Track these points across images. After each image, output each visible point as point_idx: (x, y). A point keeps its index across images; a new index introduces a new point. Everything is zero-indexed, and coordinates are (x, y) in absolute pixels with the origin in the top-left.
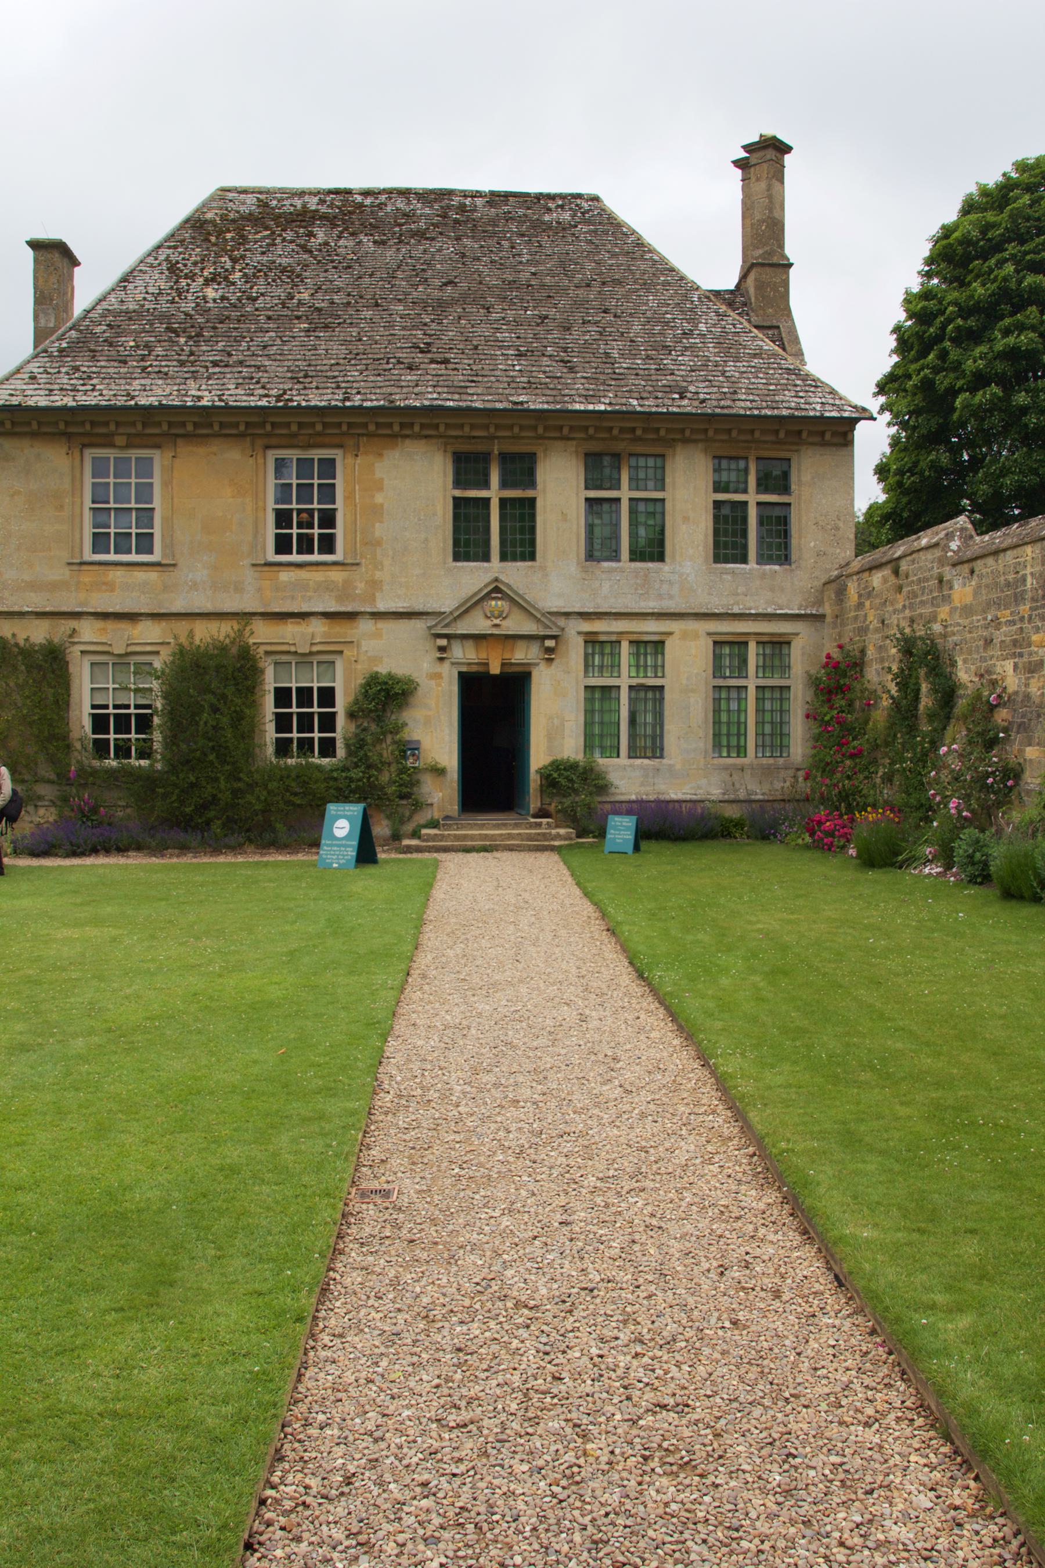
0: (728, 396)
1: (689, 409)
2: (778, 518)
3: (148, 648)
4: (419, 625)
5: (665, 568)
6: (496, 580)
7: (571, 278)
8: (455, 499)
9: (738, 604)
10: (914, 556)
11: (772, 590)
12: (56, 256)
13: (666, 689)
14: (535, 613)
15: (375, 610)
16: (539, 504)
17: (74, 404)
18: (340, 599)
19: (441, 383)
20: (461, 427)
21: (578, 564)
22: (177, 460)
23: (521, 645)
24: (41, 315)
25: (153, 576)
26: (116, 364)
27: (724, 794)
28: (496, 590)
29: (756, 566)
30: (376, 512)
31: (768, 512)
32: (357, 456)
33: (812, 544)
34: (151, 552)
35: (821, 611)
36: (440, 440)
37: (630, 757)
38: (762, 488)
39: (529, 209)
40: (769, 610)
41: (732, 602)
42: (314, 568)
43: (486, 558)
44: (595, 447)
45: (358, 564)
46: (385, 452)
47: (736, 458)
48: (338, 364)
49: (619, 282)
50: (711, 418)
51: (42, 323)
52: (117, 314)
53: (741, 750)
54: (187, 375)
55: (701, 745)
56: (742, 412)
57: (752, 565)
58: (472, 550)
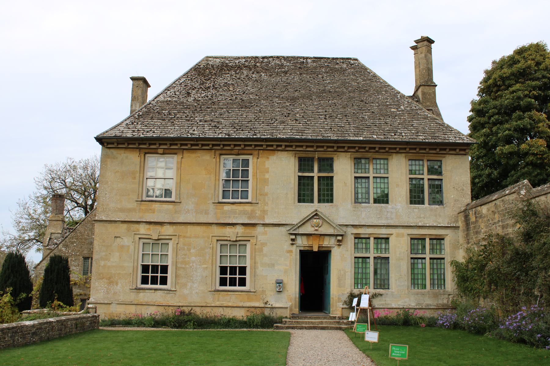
0: (414, 134)
1: (398, 140)
2: (437, 185)
3: (167, 237)
4: (283, 229)
5: (389, 206)
6: (316, 211)
7: (347, 89)
8: (299, 176)
9: (421, 222)
10: (502, 198)
11: (436, 216)
12: (141, 82)
13: (390, 259)
14: (333, 225)
15: (264, 223)
16: (335, 179)
17: (143, 136)
18: (249, 218)
19: (293, 129)
20: (302, 146)
21: (351, 203)
22: (183, 159)
23: (327, 238)
24: (134, 105)
25: (171, 206)
26: (161, 121)
27: (416, 305)
28: (316, 215)
29: (428, 205)
30: (266, 182)
31: (433, 183)
32: (258, 158)
33: (452, 196)
34: (171, 197)
35: (457, 225)
36: (293, 152)
37: (374, 289)
38: (430, 173)
39: (329, 63)
40: (435, 225)
41: (418, 221)
42: (239, 205)
43: (312, 201)
44: (358, 155)
45: (257, 203)
46: (270, 157)
47: (419, 160)
48: (251, 121)
49: (367, 90)
50: (407, 143)
51: (134, 108)
52: (163, 102)
53: (424, 286)
54: (189, 125)
55: (406, 283)
56: (421, 141)
57: (427, 204)
58: (306, 198)
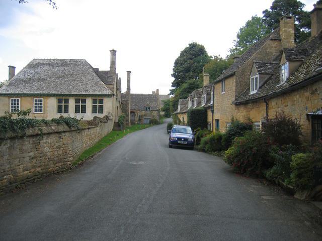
5: (85, 114)
